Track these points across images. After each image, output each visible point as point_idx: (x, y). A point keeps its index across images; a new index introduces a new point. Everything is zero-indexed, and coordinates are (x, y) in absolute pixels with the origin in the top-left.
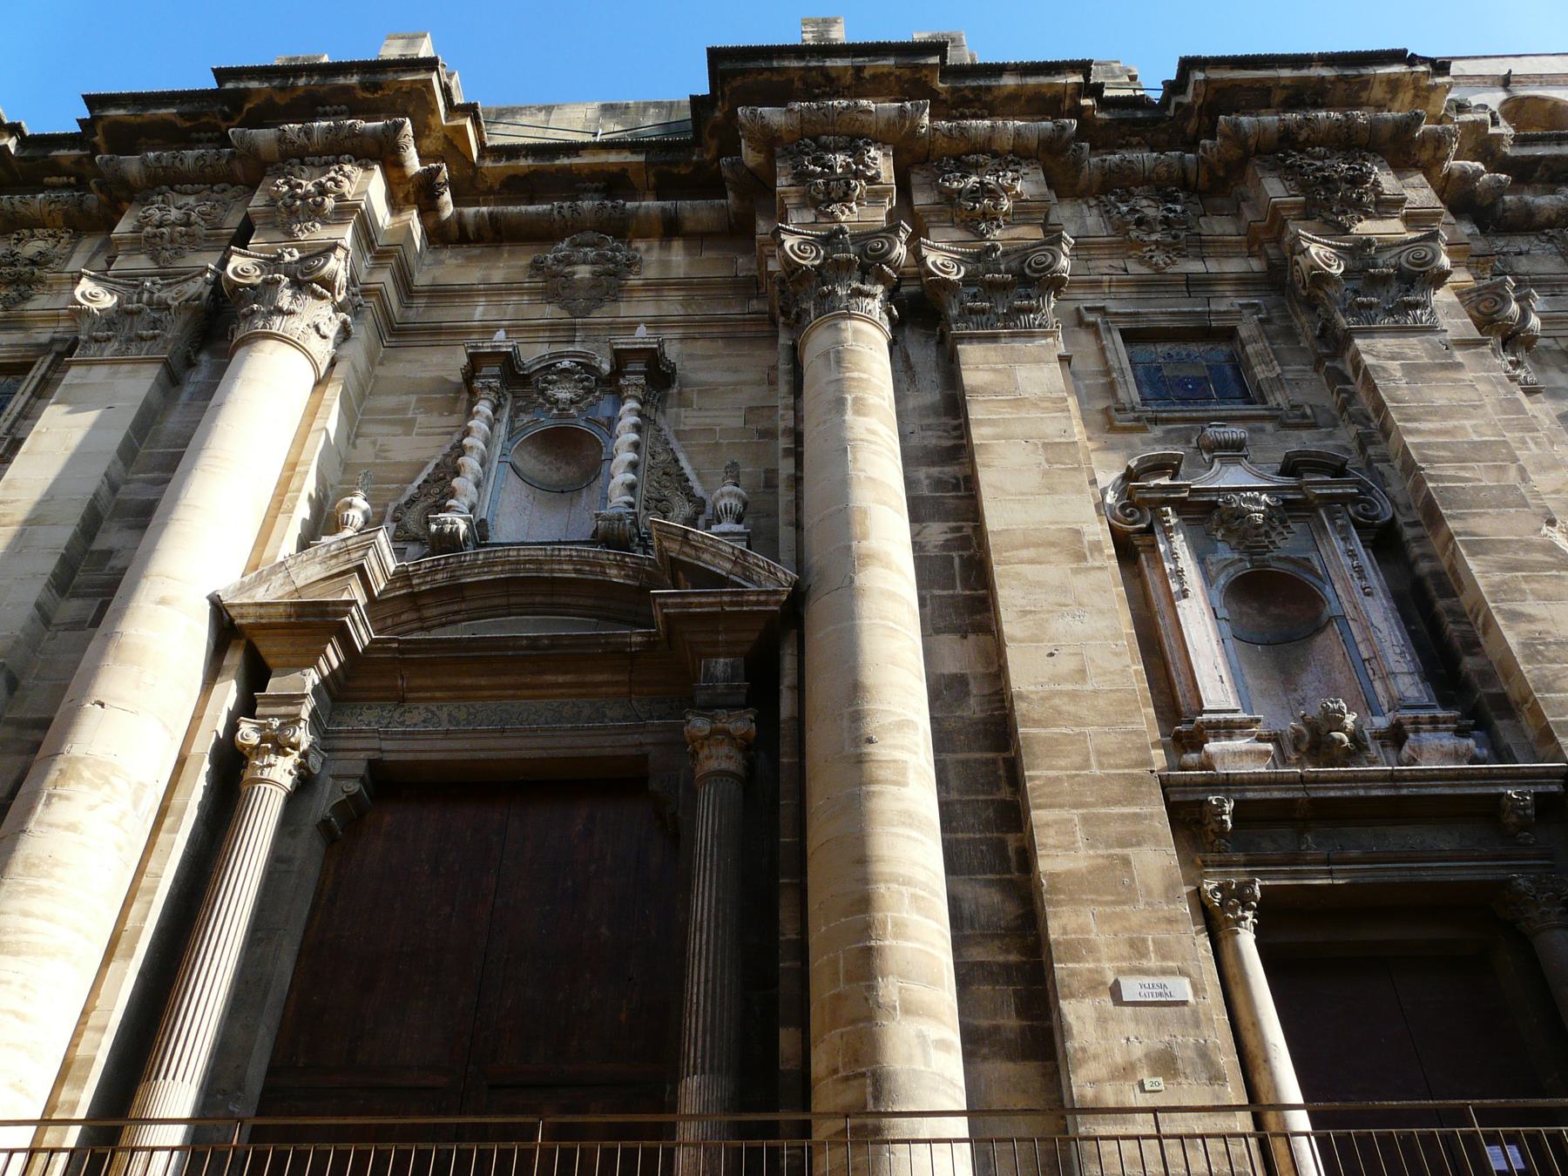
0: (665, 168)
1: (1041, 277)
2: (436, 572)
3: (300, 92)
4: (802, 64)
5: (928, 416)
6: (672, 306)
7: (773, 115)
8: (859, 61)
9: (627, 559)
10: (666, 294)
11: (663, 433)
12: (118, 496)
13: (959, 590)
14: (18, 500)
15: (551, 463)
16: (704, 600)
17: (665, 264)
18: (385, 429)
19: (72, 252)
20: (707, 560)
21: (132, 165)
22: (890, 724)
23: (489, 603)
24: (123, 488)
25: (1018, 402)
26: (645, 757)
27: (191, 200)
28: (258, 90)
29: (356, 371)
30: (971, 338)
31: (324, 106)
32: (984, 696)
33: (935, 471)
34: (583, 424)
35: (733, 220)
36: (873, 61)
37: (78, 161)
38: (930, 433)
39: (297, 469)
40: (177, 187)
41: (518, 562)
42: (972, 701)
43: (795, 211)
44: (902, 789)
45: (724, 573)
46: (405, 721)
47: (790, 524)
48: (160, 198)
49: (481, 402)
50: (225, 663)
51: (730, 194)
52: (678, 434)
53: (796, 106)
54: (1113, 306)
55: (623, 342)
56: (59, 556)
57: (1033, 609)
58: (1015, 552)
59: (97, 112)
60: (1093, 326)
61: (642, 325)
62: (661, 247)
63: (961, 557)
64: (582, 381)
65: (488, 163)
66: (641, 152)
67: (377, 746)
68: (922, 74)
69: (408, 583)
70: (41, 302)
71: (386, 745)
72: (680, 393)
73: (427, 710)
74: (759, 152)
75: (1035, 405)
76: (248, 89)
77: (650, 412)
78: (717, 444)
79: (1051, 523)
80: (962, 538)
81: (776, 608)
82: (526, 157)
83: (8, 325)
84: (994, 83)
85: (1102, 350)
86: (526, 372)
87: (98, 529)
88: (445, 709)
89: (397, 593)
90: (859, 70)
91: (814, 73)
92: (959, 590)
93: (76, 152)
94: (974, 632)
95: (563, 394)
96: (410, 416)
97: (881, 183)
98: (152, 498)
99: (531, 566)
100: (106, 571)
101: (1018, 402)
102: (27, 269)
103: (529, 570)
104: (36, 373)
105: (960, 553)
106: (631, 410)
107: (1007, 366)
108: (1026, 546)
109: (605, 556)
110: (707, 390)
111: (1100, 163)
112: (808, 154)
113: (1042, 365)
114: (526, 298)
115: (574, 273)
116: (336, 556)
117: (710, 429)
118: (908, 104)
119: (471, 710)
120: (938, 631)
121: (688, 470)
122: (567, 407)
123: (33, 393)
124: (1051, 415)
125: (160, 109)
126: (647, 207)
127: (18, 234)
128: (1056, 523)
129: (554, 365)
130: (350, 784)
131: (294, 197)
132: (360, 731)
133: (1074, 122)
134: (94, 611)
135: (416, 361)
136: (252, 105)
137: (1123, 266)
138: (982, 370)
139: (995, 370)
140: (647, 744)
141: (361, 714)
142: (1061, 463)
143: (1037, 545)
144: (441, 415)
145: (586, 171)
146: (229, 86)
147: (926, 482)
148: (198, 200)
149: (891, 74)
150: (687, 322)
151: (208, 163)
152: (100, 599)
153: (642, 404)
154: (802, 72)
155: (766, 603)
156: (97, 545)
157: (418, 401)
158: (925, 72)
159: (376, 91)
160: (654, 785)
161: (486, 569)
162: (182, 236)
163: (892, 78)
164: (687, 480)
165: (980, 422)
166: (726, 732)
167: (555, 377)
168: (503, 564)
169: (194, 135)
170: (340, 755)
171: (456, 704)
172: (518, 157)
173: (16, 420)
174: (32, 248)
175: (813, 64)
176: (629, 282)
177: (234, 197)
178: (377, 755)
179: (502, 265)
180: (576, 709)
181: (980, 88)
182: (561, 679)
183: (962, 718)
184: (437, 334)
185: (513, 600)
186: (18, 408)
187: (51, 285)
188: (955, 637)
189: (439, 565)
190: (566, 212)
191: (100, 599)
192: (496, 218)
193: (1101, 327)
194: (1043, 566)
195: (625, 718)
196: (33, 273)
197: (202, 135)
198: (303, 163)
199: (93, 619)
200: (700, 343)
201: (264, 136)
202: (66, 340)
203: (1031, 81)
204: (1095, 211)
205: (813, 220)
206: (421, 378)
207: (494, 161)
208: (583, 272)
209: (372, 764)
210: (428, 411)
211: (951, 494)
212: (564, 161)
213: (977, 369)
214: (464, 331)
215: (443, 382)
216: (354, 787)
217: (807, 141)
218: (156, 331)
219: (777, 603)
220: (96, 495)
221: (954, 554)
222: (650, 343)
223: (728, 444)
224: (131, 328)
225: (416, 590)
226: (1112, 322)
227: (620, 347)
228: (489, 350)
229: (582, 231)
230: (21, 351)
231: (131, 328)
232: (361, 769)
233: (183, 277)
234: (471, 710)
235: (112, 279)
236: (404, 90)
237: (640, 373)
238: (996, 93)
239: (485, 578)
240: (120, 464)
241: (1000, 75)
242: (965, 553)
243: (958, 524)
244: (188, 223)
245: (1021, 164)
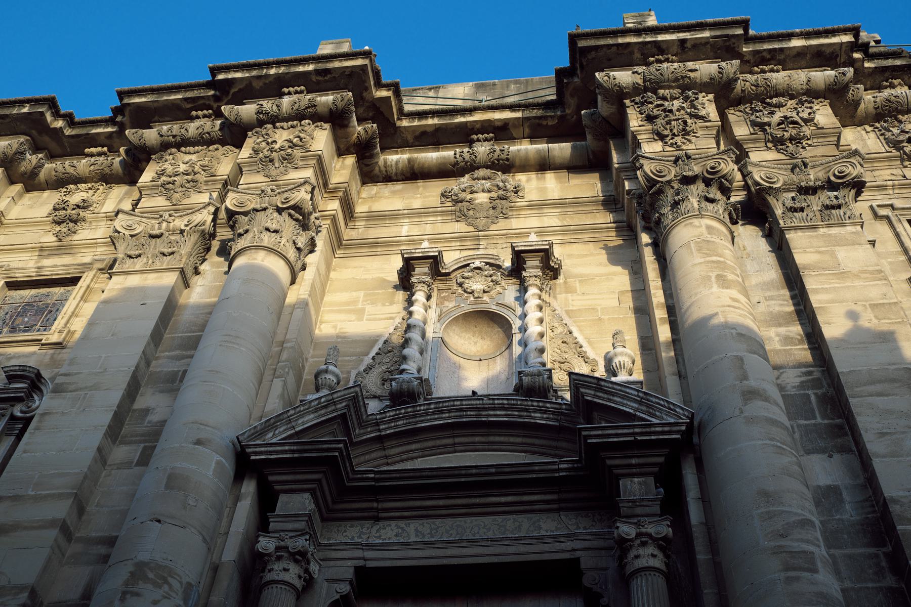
0: (537, 121)
1: (844, 182)
2: (398, 419)
3: (271, 79)
4: (640, 40)
5: (769, 289)
6: (552, 219)
7: (624, 77)
8: (682, 35)
9: (548, 405)
10: (546, 211)
11: (557, 312)
12: (151, 369)
13: (819, 420)
15: (470, 338)
16: (620, 431)
17: (543, 190)
18: (342, 316)
19: (105, 199)
20: (618, 404)
21: (150, 135)
22: (794, 522)
23: (438, 442)
24: (154, 363)
25: (843, 275)
26: (577, 560)
27: (194, 157)
28: (241, 79)
29: (320, 274)
30: (796, 228)
31: (288, 88)
32: (856, 502)
33: (782, 330)
34: (494, 307)
35: (591, 157)
36: (692, 35)
37: (110, 135)
38: (773, 302)
39: (284, 345)
40: (183, 149)
41: (461, 410)
42: (848, 507)
43: (646, 144)
44: (815, 575)
45: (632, 411)
46: (380, 536)
47: (673, 374)
48: (171, 157)
49: (417, 293)
50: (243, 490)
51: (589, 137)
52: (568, 312)
53: (640, 69)
54: (898, 204)
55: (521, 245)
56: (113, 413)
57: (888, 431)
58: (864, 388)
59: (126, 101)
60: (887, 218)
61: (533, 234)
62: (538, 178)
63: (815, 394)
64: (491, 276)
65: (405, 123)
66: (519, 110)
67: (361, 556)
68: (731, 43)
69: (377, 428)
70: (83, 234)
71: (368, 555)
72: (565, 282)
73: (398, 527)
74: (612, 104)
75: (857, 276)
76: (234, 79)
77: (545, 296)
78: (600, 319)
79: (889, 364)
80: (813, 380)
81: (678, 436)
82: (432, 117)
83: (60, 252)
84: (785, 46)
85: (897, 235)
86: (447, 271)
87: (137, 393)
88: (412, 526)
89: (368, 436)
90: (683, 42)
91: (649, 46)
92: (819, 420)
93: (109, 129)
94: (838, 452)
95: (477, 284)
96: (360, 306)
97: (710, 121)
98: (176, 369)
99: (472, 413)
100: (145, 424)
101: (843, 275)
102: (74, 212)
103: (471, 416)
104: (83, 284)
105: (815, 391)
106: (534, 295)
107: (828, 248)
108: (873, 383)
109: (530, 403)
110: (585, 279)
111: (873, 99)
112: (651, 103)
113: (856, 246)
114: (439, 218)
115: (475, 199)
116: (325, 407)
117: (593, 309)
118: (724, 64)
119: (433, 526)
120: (808, 452)
121: (581, 339)
122: (480, 295)
123: (82, 298)
124: (871, 283)
125: (170, 96)
126: (526, 149)
127: (67, 188)
128: (893, 364)
129: (468, 265)
130: (342, 586)
131: (272, 150)
132: (346, 544)
133: (852, 70)
134: (138, 454)
135: (361, 267)
136: (236, 90)
137: (902, 174)
138: (808, 252)
139: (819, 252)
140: (578, 550)
141: (345, 531)
142: (889, 319)
143: (880, 382)
144: (384, 305)
145: (478, 126)
146: (220, 77)
147: (777, 339)
148: (198, 157)
149: (707, 43)
150: (564, 230)
152: (142, 445)
153: (541, 290)
154: (641, 46)
155: (669, 432)
156: (136, 406)
157: (365, 295)
158: (733, 40)
160: (586, 581)
161: (436, 416)
163: (709, 46)
164: (581, 347)
165: (816, 291)
166: (649, 535)
167: (469, 274)
168: (449, 411)
169: (194, 113)
170: (332, 563)
171: (421, 522)
172: (427, 118)
173: (70, 317)
174: (76, 198)
175: (649, 39)
176: (518, 204)
177: (224, 154)
178: (361, 563)
179: (419, 196)
180: (517, 524)
181: (775, 49)
182: (503, 499)
183: (842, 520)
184: (374, 246)
185: (457, 440)
186: (71, 309)
187: (91, 222)
188: (825, 456)
189: (400, 414)
190: (467, 156)
191: (142, 445)
192: (413, 161)
193: (894, 219)
194: (890, 397)
195: (557, 529)
196: (79, 215)
198: (275, 127)
199: (138, 460)
200: (575, 245)
201: (248, 110)
202: (104, 260)
203: (814, 42)
204: (872, 135)
205: (662, 149)
206: (366, 279)
207: (410, 122)
208: (482, 198)
209: (358, 570)
210: (373, 303)
211: (799, 347)
212: (460, 119)
213: (805, 252)
214: (398, 244)
215: (383, 282)
216: (345, 588)
217: (649, 94)
218: (174, 249)
219: (677, 432)
220: (137, 367)
221: (810, 392)
222: (543, 245)
223: (609, 319)
224: (155, 247)
225: (383, 433)
226: (901, 215)
227: (520, 249)
228: (420, 255)
229: (478, 168)
230: (71, 269)
231: (155, 247)
232: (350, 574)
233: (191, 211)
234: (433, 526)
235: (139, 214)
237: (537, 267)
238: (788, 52)
239: (436, 423)
240: (152, 345)
241: (790, 40)
242: (819, 392)
243: (808, 369)
245: (813, 103)
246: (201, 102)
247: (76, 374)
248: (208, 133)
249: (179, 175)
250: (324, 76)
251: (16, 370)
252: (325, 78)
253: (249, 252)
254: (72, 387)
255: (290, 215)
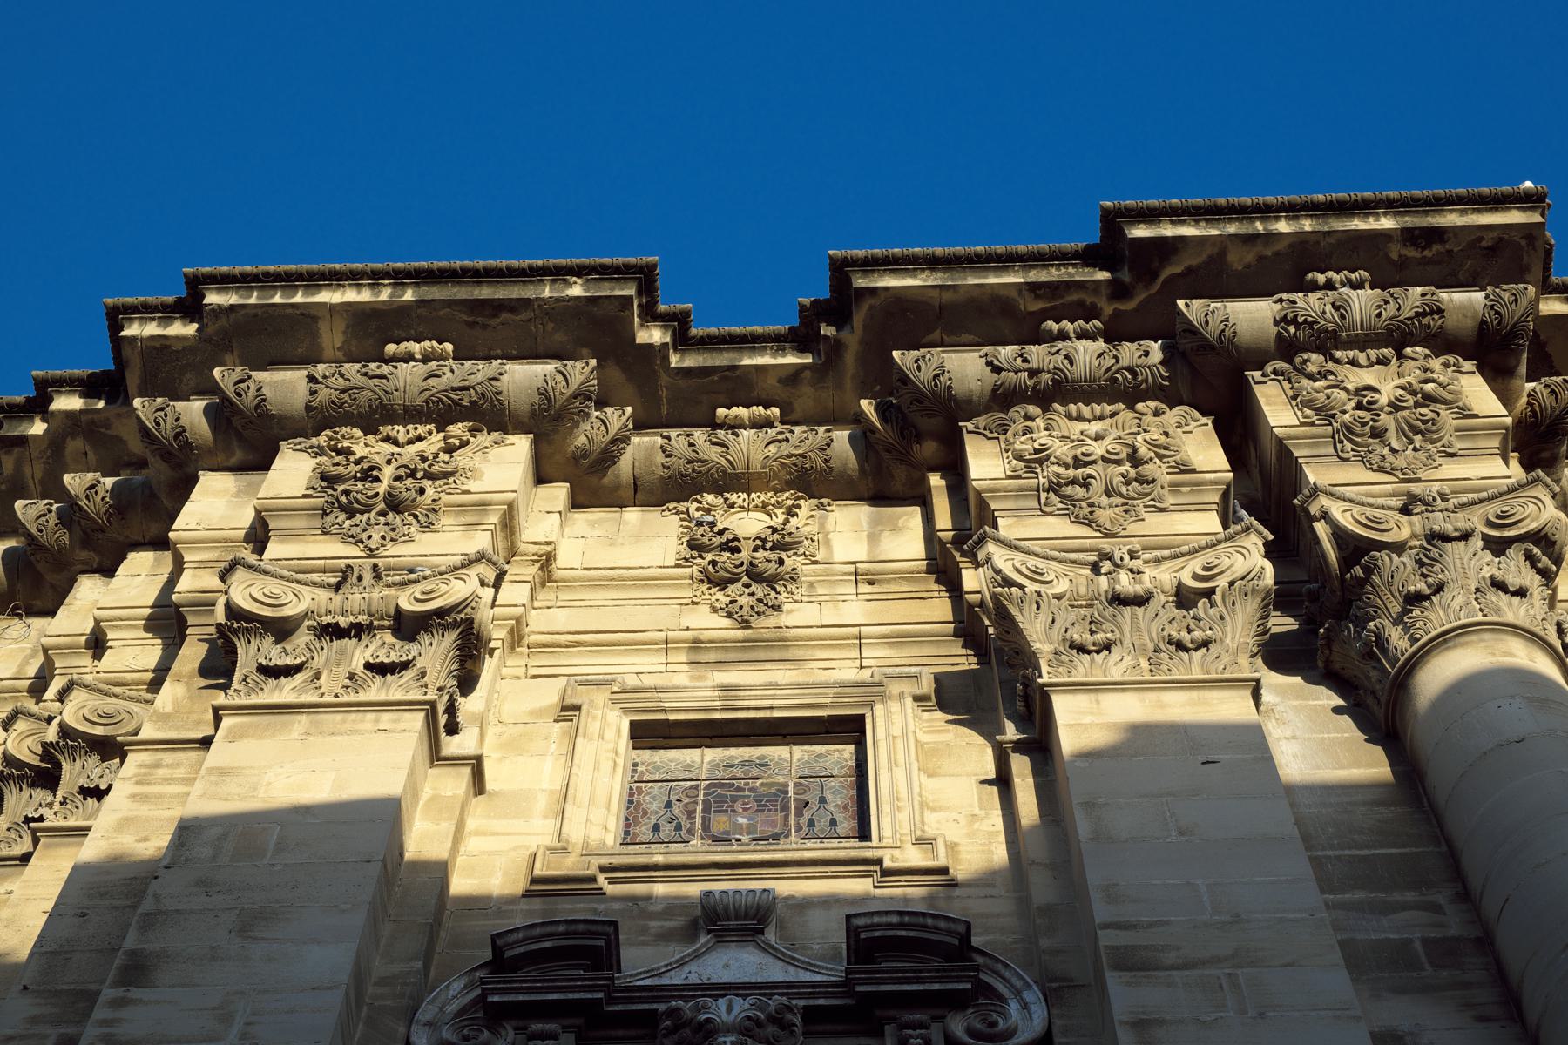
3: (1281, 246)
14: (1168, 923)
37: (793, 377)
93: (791, 359)
125: (986, 277)
136: (1177, 269)
151: (1125, 362)
159: (1428, 246)
162: (1128, 483)
169: (1052, 326)
187: (811, 585)
197: (1068, 326)
233: (1166, 553)
236: (1484, 244)
244: (1135, 460)
246: (1073, 297)
247: (1151, 925)
248: (1131, 369)
249: (1093, 462)
250: (1424, 248)
251: (890, 926)
252: (1426, 253)
253: (1474, 637)
254: (1169, 958)
255: (1530, 557)
